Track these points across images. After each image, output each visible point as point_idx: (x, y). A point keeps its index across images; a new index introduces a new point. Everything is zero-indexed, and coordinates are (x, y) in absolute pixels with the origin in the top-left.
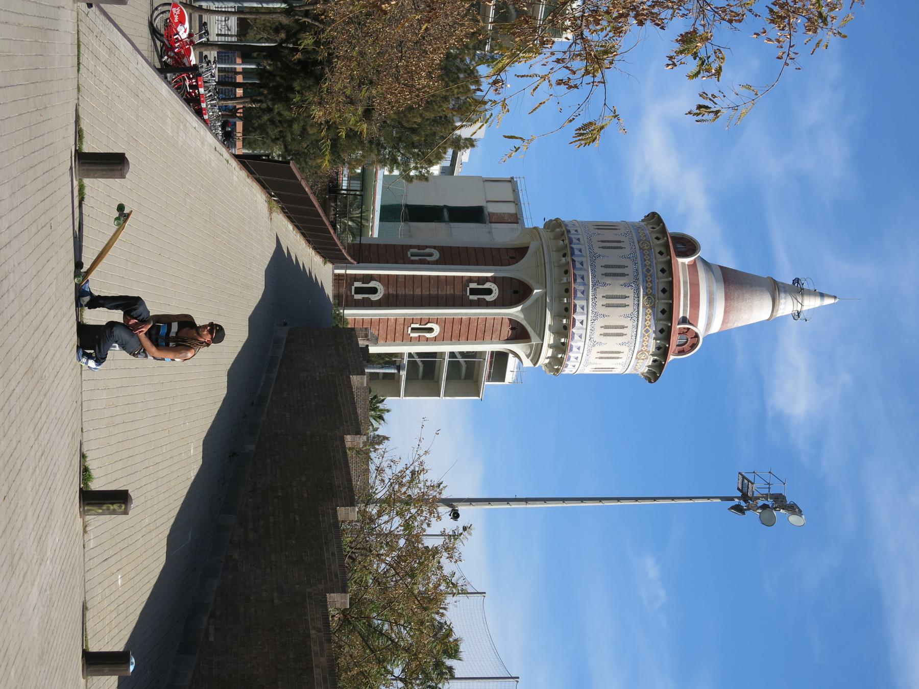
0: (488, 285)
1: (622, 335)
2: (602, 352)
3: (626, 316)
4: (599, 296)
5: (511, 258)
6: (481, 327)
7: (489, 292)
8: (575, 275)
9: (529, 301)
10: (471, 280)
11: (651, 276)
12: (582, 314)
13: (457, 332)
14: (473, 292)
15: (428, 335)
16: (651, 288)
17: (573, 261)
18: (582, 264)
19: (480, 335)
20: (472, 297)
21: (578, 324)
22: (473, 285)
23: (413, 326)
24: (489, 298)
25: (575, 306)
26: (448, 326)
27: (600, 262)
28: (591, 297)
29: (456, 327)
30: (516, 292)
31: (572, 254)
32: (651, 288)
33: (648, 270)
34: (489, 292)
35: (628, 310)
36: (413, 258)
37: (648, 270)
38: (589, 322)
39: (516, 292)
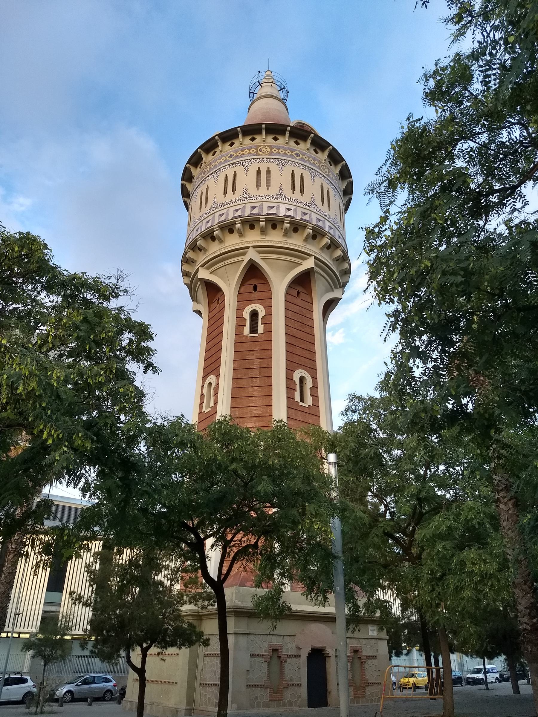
0: (246, 315)
1: (302, 178)
2: (323, 201)
3: (281, 170)
4: (258, 193)
5: (218, 303)
6: (297, 325)
7: (254, 314)
8: (234, 218)
9: (263, 264)
10: (239, 333)
12: (278, 207)
13: (304, 352)
14: (254, 329)
15: (309, 383)
16: (250, 150)
18: (221, 215)
19: (307, 330)
20: (261, 329)
21: (291, 213)
22: (246, 330)
23: (297, 398)
24: (262, 313)
26: (296, 359)
27: (221, 199)
28: (259, 200)
29: (298, 351)
30: (255, 288)
32: (250, 150)
34: (254, 314)
35: (274, 168)
36: (212, 404)
37: (231, 156)
38: (288, 202)
39: (255, 288)
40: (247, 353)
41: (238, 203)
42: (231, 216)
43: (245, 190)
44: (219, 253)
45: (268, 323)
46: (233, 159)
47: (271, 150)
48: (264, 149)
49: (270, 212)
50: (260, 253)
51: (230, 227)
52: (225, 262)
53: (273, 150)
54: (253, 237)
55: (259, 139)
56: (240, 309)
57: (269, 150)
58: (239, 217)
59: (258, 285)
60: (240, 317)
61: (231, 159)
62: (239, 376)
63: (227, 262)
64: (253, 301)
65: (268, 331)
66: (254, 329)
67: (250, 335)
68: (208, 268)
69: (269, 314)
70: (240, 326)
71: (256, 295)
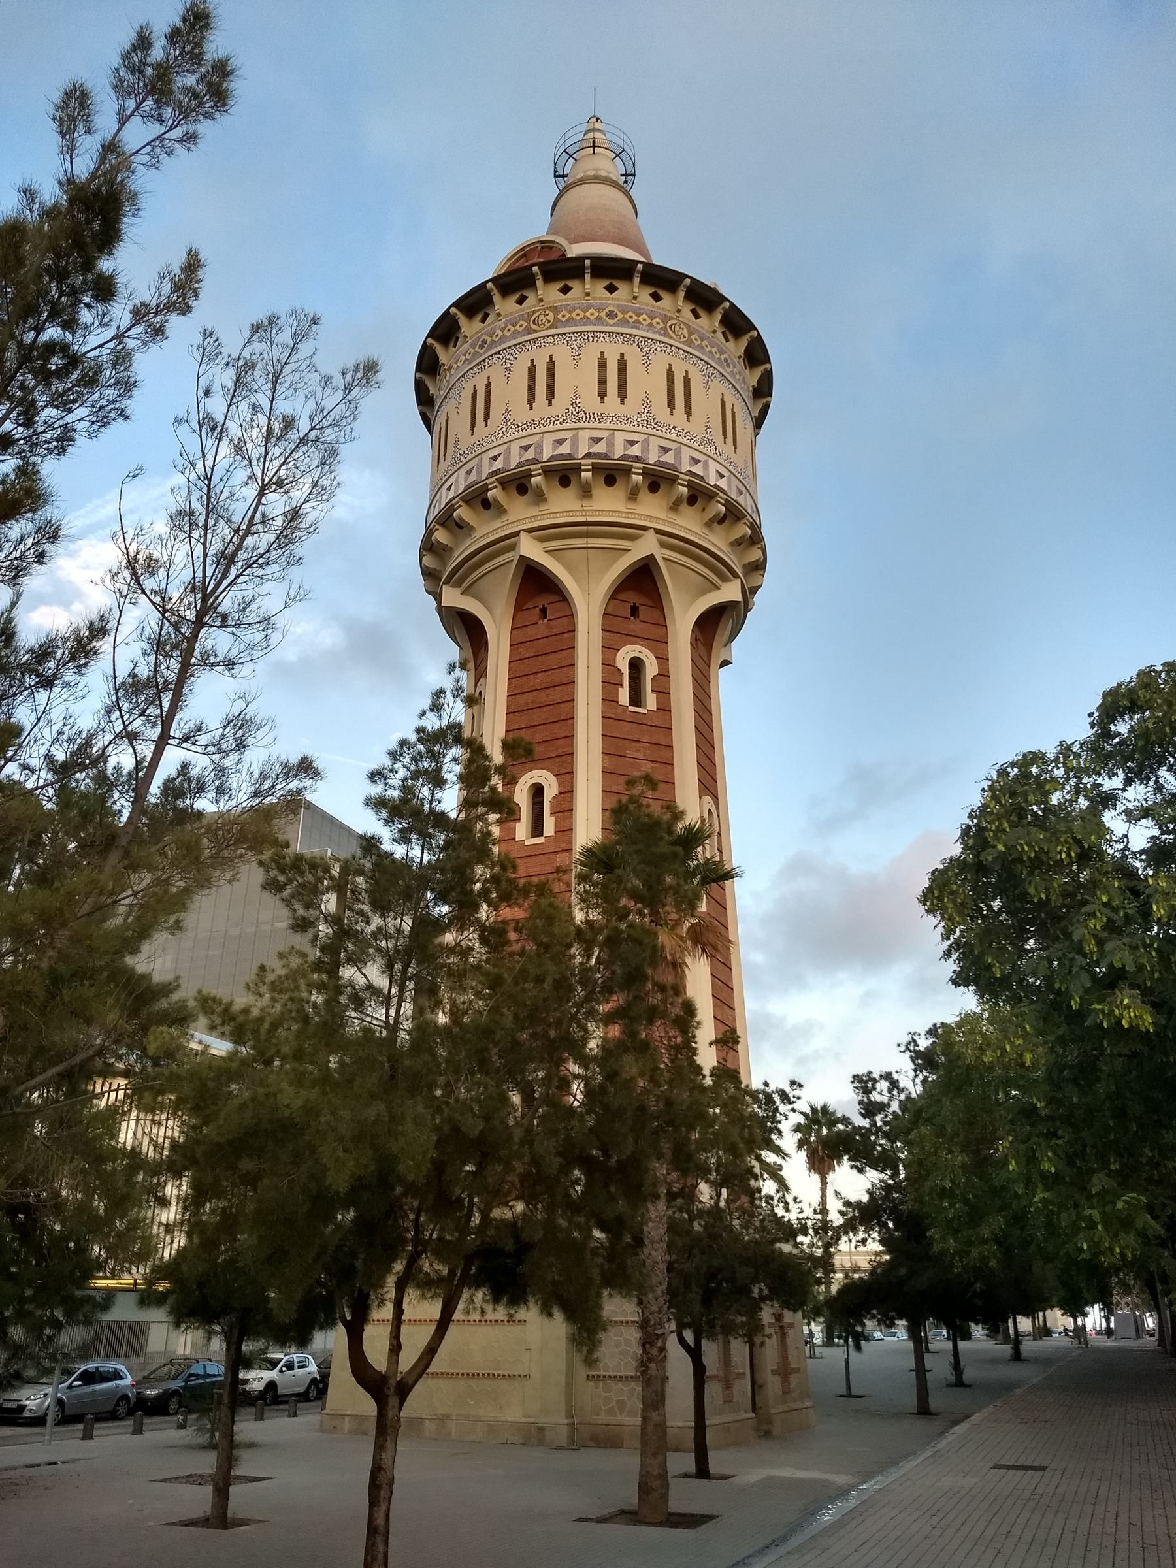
7: (636, 665)
8: (624, 457)
10: (609, 700)
11: (624, 312)
14: (636, 698)
17: (588, 456)
18: (597, 440)
20: (651, 701)
22: (624, 696)
24: (651, 669)
25: (691, 473)
30: (634, 611)
31: (570, 456)
33: (611, 315)
34: (636, 665)
37: (611, 315)
39: (634, 611)
40: (627, 744)
41: (632, 428)
42: (618, 452)
43: (646, 403)
44: (583, 519)
45: (663, 693)
46: (614, 325)
47: (690, 334)
48: (677, 328)
49: (693, 469)
50: (663, 545)
51: (613, 473)
52: (591, 540)
53: (693, 337)
54: (651, 510)
55: (667, 302)
56: (610, 649)
57: (685, 332)
58: (638, 459)
59: (641, 608)
60: (609, 665)
61: (612, 322)
62: (614, 789)
63: (593, 542)
64: (633, 638)
65: (664, 708)
66: (636, 698)
67: (631, 708)
68: (542, 540)
69: (663, 675)
70: (610, 683)
71: (635, 626)
